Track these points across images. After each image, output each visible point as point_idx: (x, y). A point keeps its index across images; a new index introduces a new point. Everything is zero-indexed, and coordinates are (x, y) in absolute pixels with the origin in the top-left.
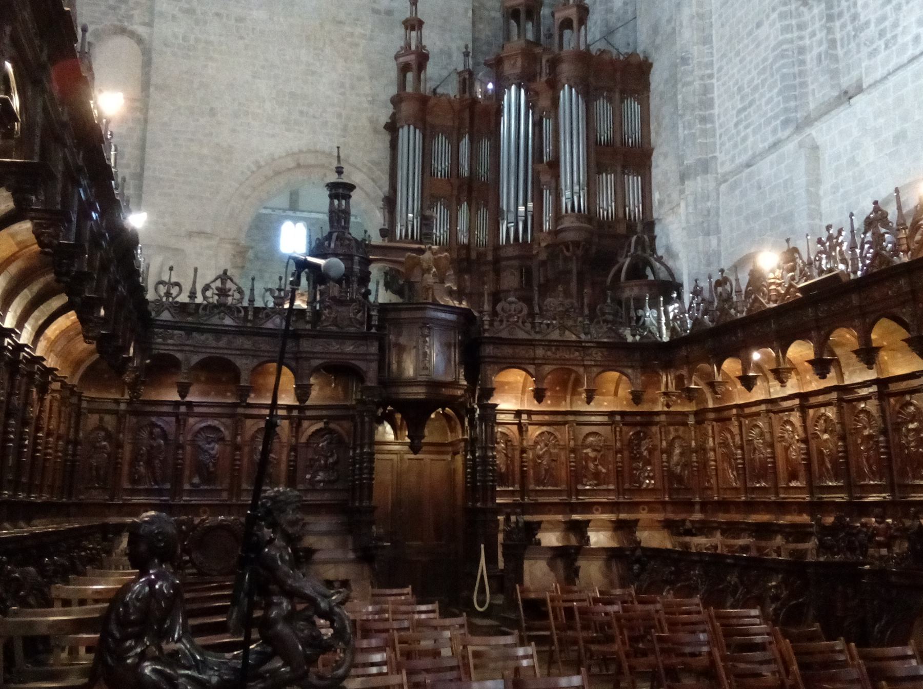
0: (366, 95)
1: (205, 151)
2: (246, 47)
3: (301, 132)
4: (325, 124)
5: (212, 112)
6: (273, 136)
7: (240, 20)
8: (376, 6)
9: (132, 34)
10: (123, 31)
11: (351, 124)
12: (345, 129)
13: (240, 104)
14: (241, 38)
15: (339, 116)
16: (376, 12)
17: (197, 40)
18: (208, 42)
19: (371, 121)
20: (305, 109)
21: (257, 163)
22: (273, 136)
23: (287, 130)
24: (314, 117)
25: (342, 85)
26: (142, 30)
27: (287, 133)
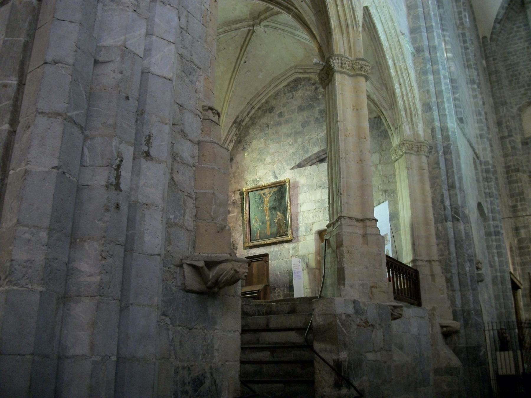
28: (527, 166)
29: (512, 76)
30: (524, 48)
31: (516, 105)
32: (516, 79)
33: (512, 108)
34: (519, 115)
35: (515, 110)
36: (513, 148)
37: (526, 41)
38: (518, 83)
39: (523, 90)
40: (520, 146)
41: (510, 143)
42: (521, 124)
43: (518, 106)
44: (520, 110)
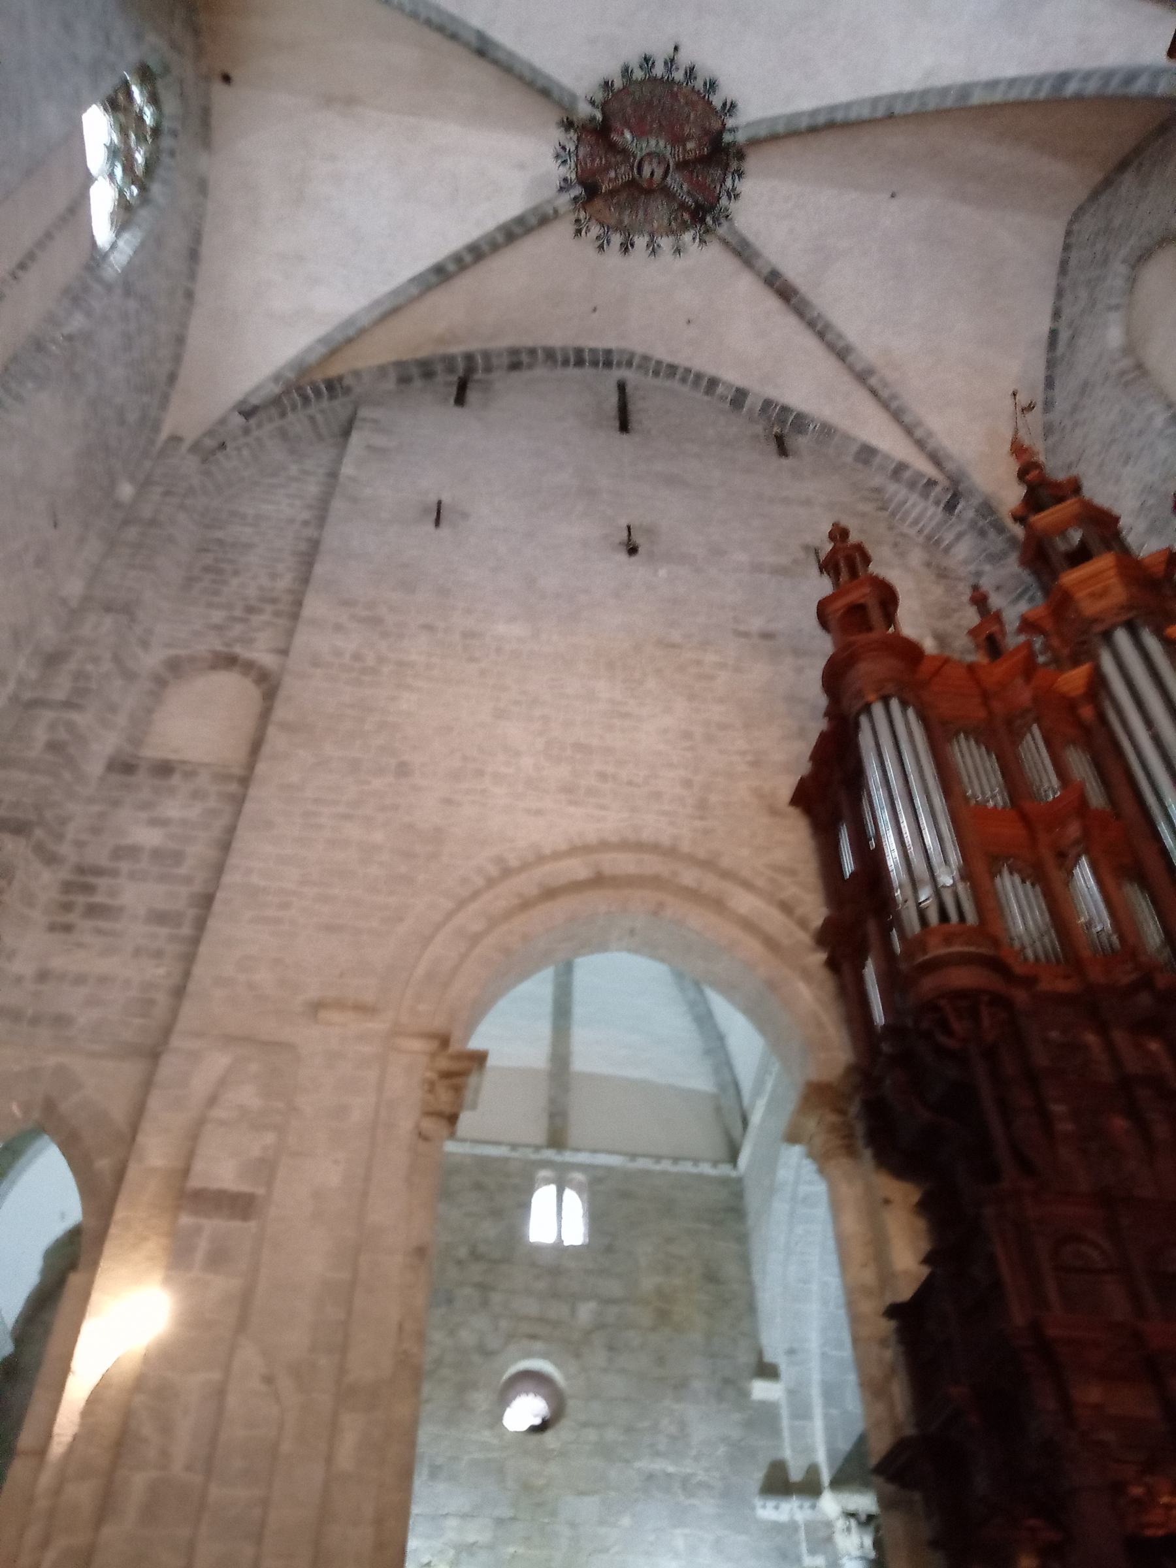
0: (743, 753)
1: (378, 836)
2: (483, 673)
3: (603, 807)
4: (657, 796)
5: (403, 770)
6: (539, 812)
7: (468, 635)
8: (742, 628)
9: (248, 667)
10: (229, 661)
11: (714, 798)
12: (702, 806)
13: (465, 758)
14: (472, 659)
15: (687, 783)
16: (746, 635)
17: (381, 660)
18: (401, 664)
19: (758, 793)
20: (610, 769)
21: (499, 860)
22: (539, 812)
23: (571, 803)
24: (630, 783)
25: (687, 735)
26: (267, 660)
27: (572, 809)
28: (80, 844)
29: (207, 569)
30: (291, 521)
31: (168, 645)
32: (214, 581)
33: (145, 644)
34: (161, 682)
35: (151, 660)
36: (53, 746)
37: (310, 507)
38: (216, 593)
39: (218, 616)
40: (95, 768)
41: (52, 727)
42: (150, 711)
43: (172, 652)
44: (176, 667)
